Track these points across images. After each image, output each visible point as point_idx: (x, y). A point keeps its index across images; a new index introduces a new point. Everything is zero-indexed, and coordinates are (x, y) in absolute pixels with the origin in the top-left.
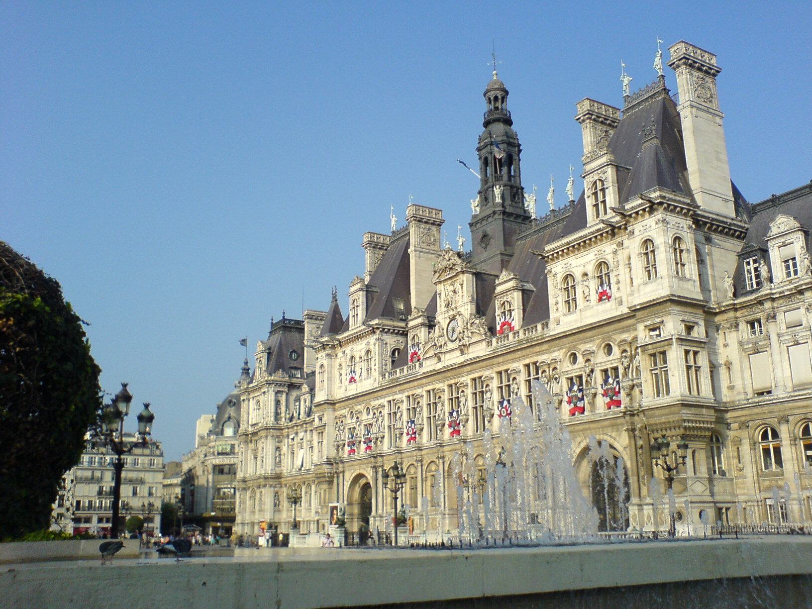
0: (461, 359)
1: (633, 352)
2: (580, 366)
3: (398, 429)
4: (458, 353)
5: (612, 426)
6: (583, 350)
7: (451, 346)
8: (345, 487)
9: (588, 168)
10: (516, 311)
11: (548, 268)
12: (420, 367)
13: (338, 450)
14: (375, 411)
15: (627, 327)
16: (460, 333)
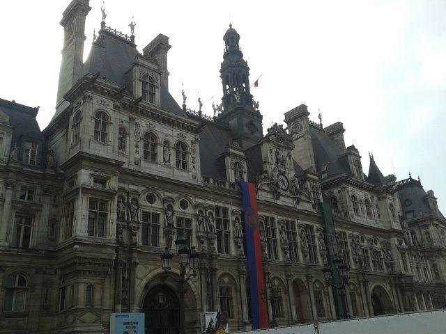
0: (299, 207)
4: (291, 201)
7: (283, 192)
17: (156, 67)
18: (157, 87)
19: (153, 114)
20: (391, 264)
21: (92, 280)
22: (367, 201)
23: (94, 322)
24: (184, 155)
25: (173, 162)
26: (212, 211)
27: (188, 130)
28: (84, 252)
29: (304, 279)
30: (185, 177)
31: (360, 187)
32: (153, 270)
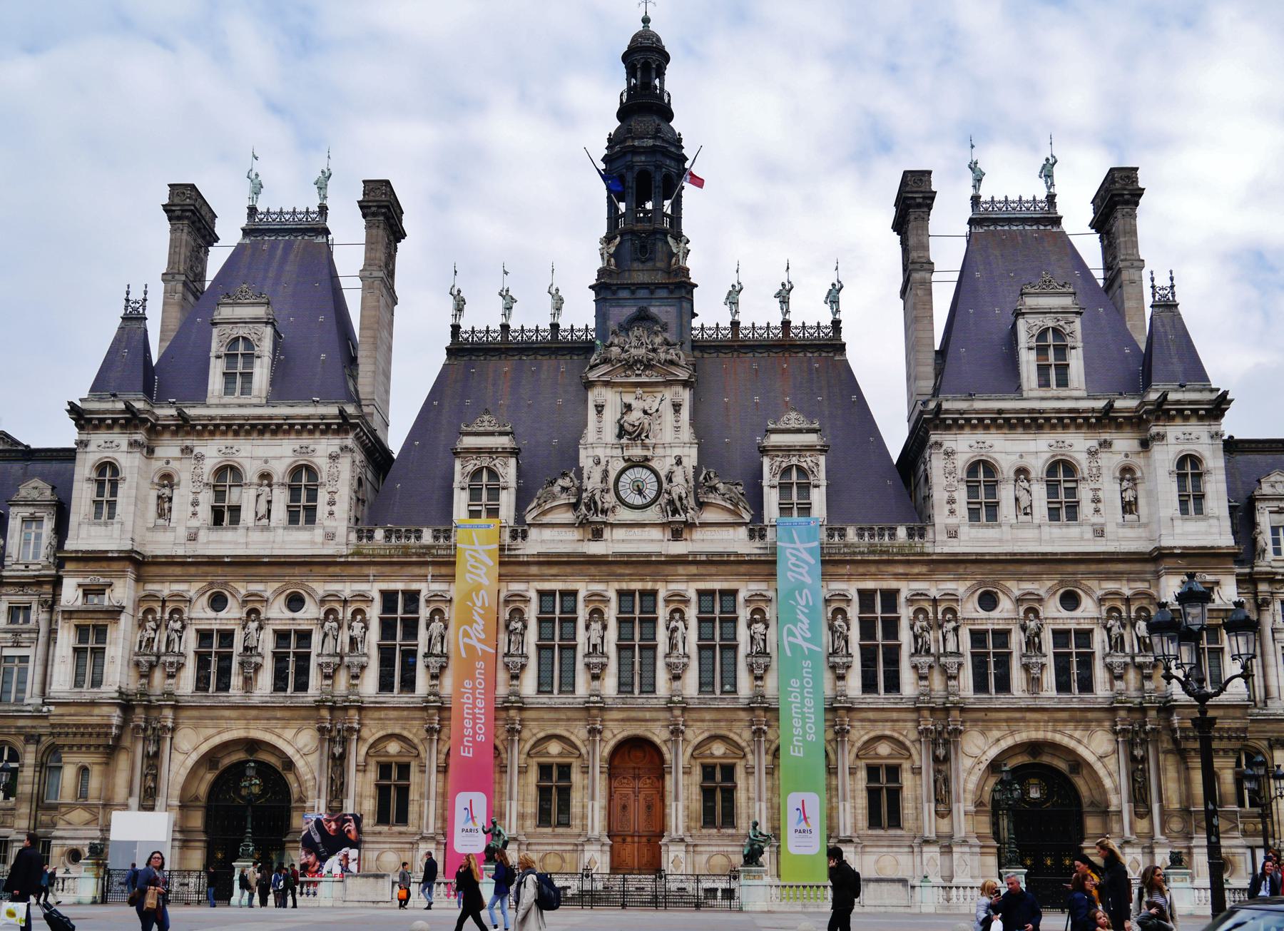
0: (678, 548)
1: (1133, 614)
2: (1006, 615)
3: (437, 656)
4: (656, 533)
5: (1078, 721)
6: (1017, 593)
7: (624, 515)
8: (174, 767)
9: (1031, 302)
10: (823, 489)
11: (934, 438)
12: (514, 535)
13: (146, 674)
14: (338, 606)
15: (1116, 573)
16: (680, 498)
17: (260, 312)
18: (258, 357)
19: (229, 426)
20: (1140, 667)
21: (85, 759)
22: (1061, 469)
23: (86, 824)
24: (313, 495)
25: (280, 513)
26: (363, 606)
27: (323, 432)
28: (62, 715)
29: (659, 734)
30: (303, 542)
31: (1033, 422)
32: (213, 736)
